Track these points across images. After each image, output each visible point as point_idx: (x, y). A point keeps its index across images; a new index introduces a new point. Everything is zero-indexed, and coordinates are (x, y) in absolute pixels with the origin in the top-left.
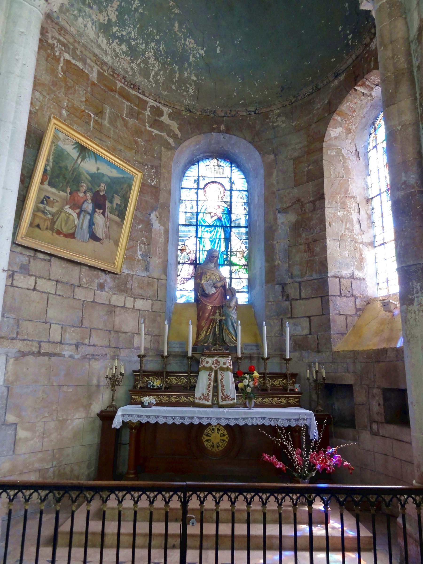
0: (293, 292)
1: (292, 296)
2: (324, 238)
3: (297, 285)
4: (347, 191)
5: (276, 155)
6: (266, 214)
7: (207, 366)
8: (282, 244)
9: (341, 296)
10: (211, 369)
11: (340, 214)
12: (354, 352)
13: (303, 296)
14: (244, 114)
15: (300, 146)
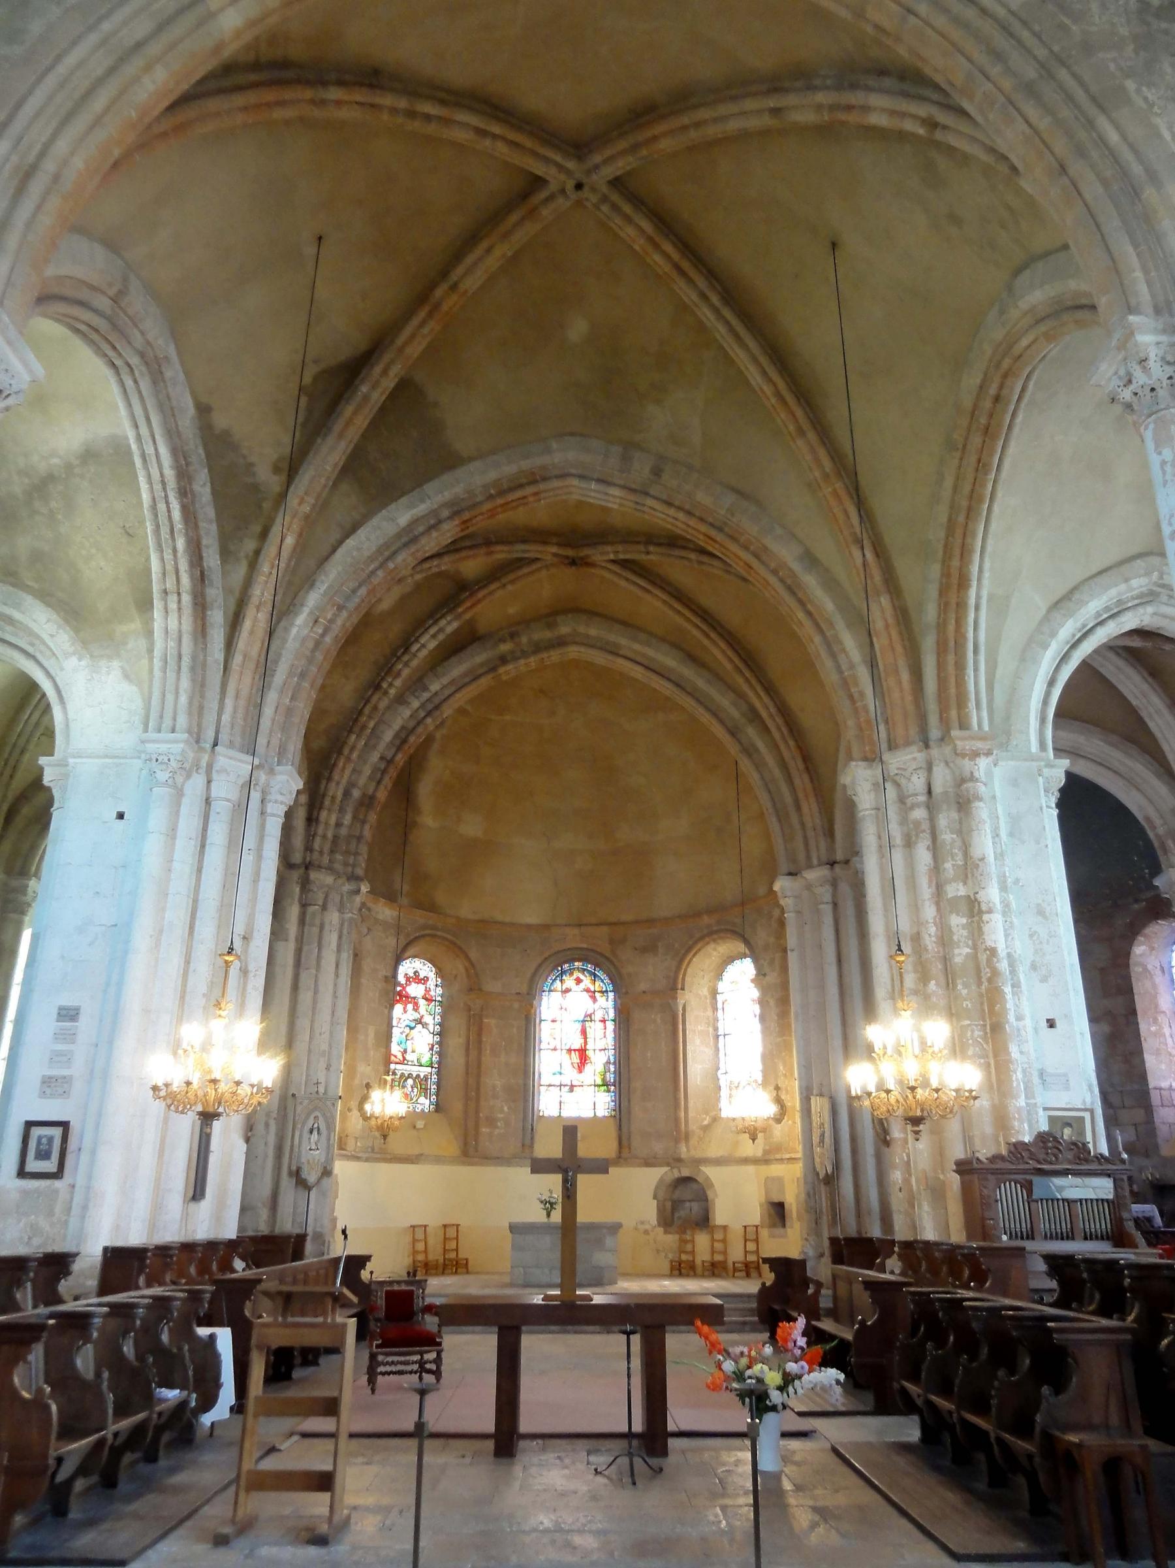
2: (1140, 1052)
4: (1157, 1006)
11: (1153, 1029)
13: (1126, 1104)
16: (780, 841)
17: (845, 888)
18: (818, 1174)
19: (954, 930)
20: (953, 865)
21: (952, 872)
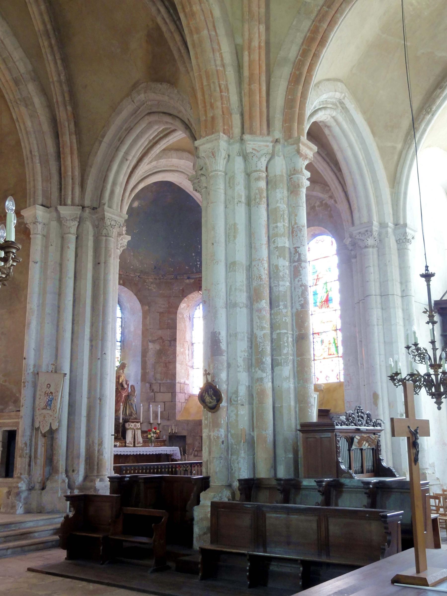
0: (156, 388)
1: (155, 390)
2: (175, 362)
3: (158, 384)
4: (185, 338)
5: (149, 307)
6: (143, 341)
7: (132, 427)
8: (151, 361)
9: (180, 393)
10: (133, 429)
11: (182, 350)
12: (188, 421)
13: (161, 391)
14: (133, 276)
15: (163, 306)
16: (39, 178)
17: (89, 227)
18: (38, 429)
19: (281, 269)
20: (284, 225)
21: (282, 229)
